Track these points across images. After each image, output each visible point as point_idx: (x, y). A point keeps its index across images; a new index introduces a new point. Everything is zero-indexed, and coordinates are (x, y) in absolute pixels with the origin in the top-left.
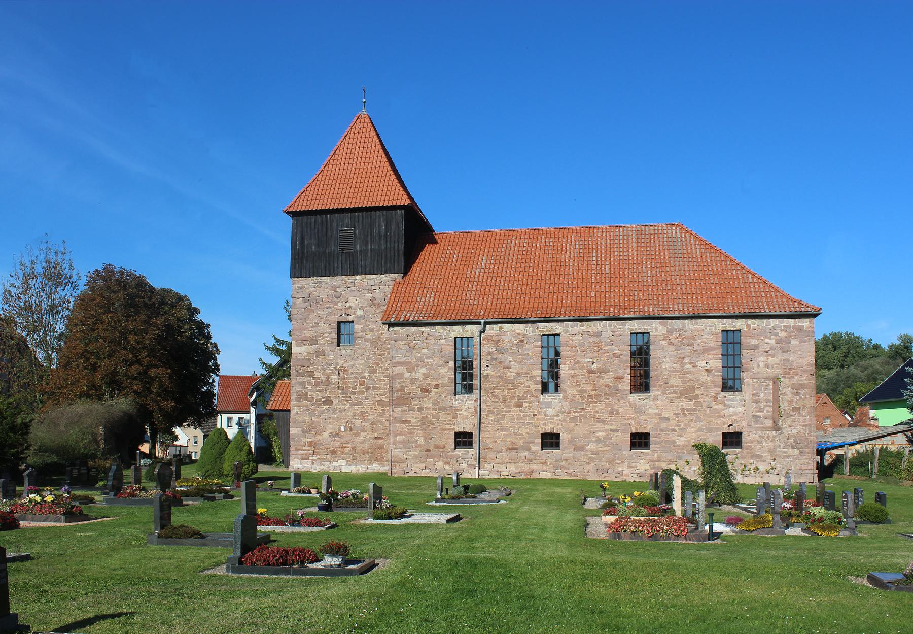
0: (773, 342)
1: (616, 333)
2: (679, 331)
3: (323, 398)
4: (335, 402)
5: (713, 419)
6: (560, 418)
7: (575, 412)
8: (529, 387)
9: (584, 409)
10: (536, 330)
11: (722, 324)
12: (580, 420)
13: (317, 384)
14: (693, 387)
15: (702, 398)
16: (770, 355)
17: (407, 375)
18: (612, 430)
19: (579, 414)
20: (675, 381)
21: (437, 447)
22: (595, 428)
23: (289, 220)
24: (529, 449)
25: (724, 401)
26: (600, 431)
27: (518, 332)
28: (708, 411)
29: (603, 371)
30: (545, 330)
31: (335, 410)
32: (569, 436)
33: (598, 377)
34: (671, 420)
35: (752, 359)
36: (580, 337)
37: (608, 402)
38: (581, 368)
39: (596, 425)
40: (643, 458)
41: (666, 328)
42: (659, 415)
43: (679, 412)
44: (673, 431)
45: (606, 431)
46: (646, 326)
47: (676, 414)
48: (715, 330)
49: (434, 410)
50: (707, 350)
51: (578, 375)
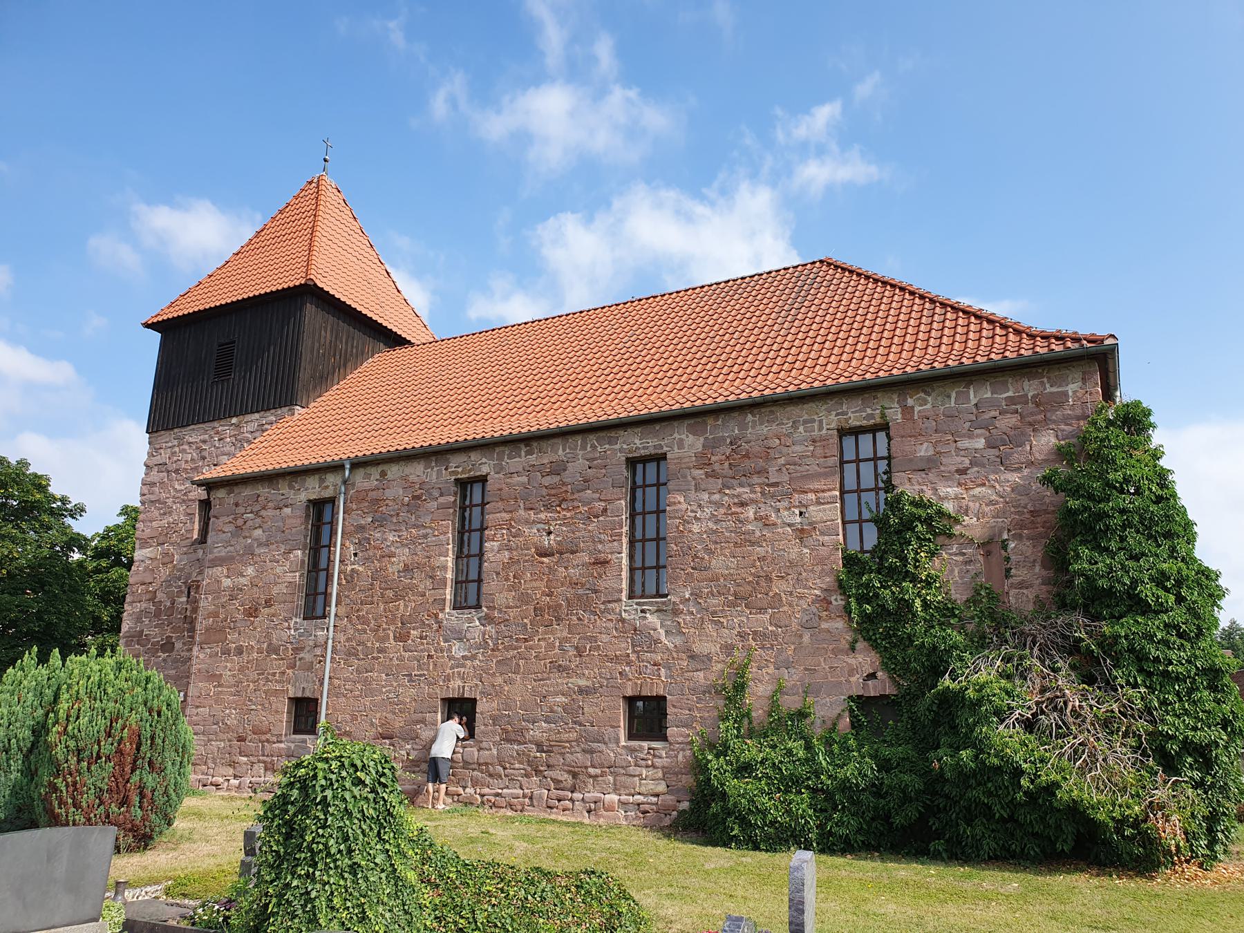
0: (980, 443)
1: (595, 462)
2: (731, 443)
3: (162, 640)
4: (178, 645)
5: (822, 660)
10: (444, 472)
11: (837, 415)
13: (157, 614)
14: (769, 579)
17: (227, 582)
18: (582, 691)
23: (156, 337)
27: (412, 478)
29: (566, 550)
30: (460, 470)
32: (495, 705)
36: (525, 479)
39: (549, 679)
41: (702, 439)
46: (659, 440)
48: (820, 429)
49: (260, 651)
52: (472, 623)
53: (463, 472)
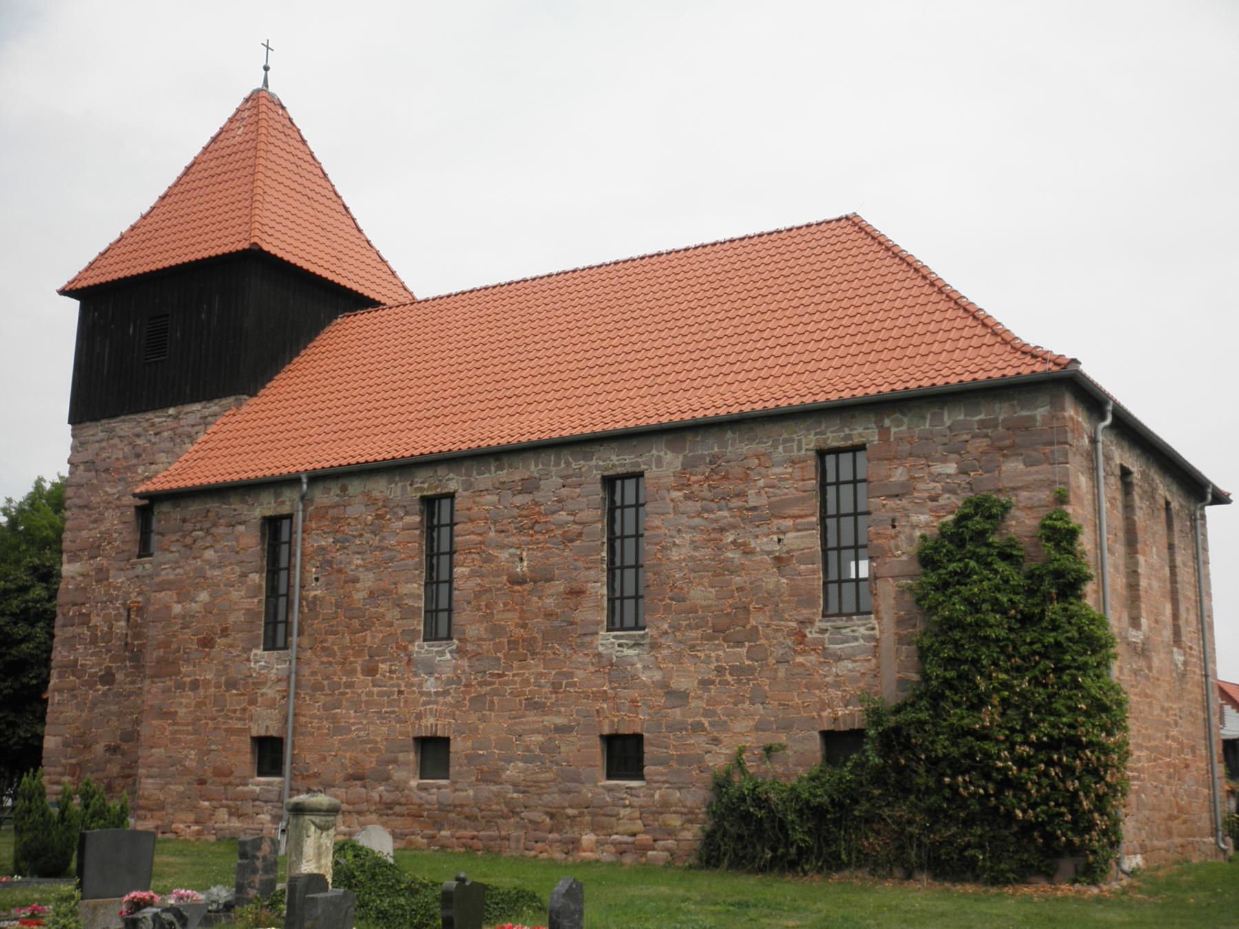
0: (951, 468)
1: (570, 480)
2: (711, 463)
3: (101, 670)
4: (119, 676)
5: (795, 694)
6: (449, 699)
7: (480, 684)
8: (391, 625)
9: (499, 676)
10: (409, 488)
11: (816, 434)
12: (492, 702)
13: (94, 641)
14: (746, 609)
15: (767, 637)
16: (943, 507)
17: (177, 609)
18: (559, 729)
19: (489, 688)
20: (702, 594)
21: (218, 773)
22: (522, 723)
23: (75, 304)
24: (387, 778)
25: (822, 642)
26: (533, 732)
27: (376, 494)
28: (781, 674)
29: (541, 577)
30: (426, 486)
31: (118, 695)
32: (469, 744)
33: (531, 592)
34: (693, 698)
35: (893, 520)
37: (552, 656)
38: (497, 574)
39: (524, 716)
40: (627, 802)
41: (681, 458)
42: (664, 685)
43: (712, 676)
44: (697, 727)
45: (544, 731)
46: (637, 457)
47: (705, 684)
48: (799, 449)
49: (218, 686)
50: (777, 510)
51: (489, 590)
52: (444, 656)
53: (429, 489)
